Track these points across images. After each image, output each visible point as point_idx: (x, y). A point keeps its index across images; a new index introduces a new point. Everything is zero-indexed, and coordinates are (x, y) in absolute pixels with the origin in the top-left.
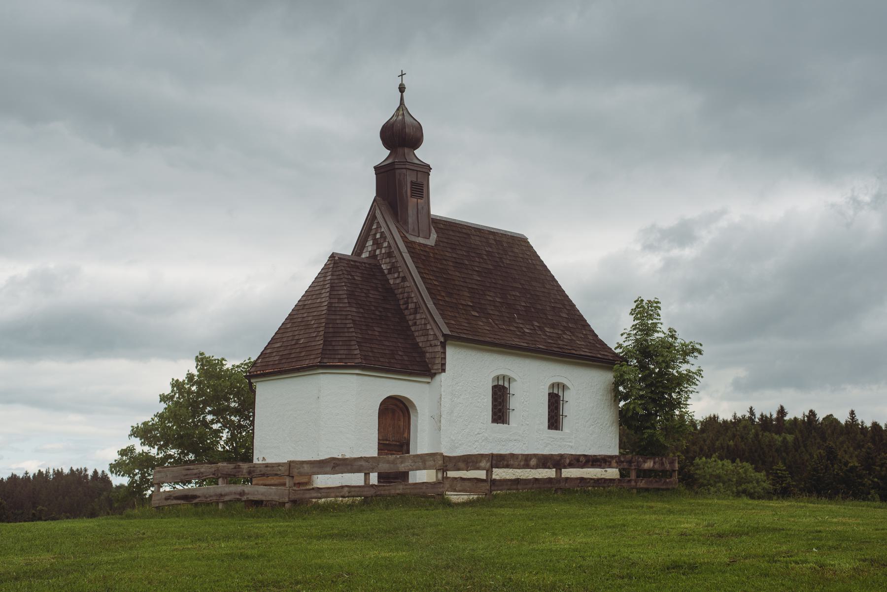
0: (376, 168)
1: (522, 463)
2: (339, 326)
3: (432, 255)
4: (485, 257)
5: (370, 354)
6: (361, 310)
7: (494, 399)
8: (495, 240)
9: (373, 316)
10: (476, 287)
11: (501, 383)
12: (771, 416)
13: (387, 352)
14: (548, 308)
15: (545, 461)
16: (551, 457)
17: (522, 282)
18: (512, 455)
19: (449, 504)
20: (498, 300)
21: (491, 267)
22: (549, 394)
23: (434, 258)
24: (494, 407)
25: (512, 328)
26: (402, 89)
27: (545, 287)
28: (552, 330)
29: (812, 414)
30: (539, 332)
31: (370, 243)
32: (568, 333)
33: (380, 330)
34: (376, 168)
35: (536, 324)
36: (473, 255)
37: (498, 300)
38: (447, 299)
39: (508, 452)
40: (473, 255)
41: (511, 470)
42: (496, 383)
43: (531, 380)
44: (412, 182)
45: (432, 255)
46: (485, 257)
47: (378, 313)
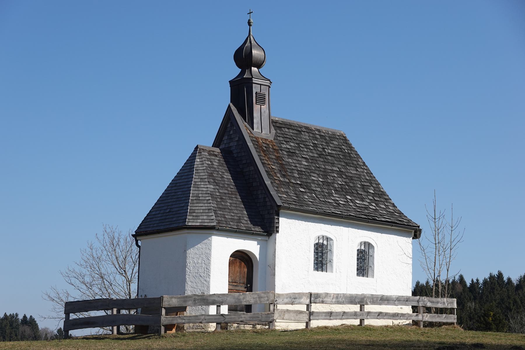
0: (229, 82)
1: (334, 300)
2: (201, 198)
3: (271, 147)
4: (311, 148)
5: (223, 219)
6: (217, 187)
7: (316, 252)
8: (320, 135)
9: (226, 192)
10: (304, 170)
11: (321, 241)
12: (427, 283)
13: (236, 218)
14: (359, 186)
15: (352, 300)
16: (356, 296)
17: (340, 166)
18: (327, 294)
19: (70, 337)
20: (321, 180)
21: (316, 155)
22: (358, 250)
23: (273, 148)
24: (316, 259)
25: (330, 201)
26: (249, 23)
27: (357, 170)
28: (361, 202)
29: (500, 275)
30: (351, 204)
31: (226, 137)
32: (374, 204)
33: (231, 202)
34: (229, 82)
35: (349, 197)
36: (302, 146)
37: (321, 180)
38: (281, 179)
39: (324, 292)
40: (302, 146)
41: (296, 309)
42: (317, 242)
43: (346, 240)
44: (256, 93)
45: (271, 147)
46: (311, 148)
47: (229, 189)
